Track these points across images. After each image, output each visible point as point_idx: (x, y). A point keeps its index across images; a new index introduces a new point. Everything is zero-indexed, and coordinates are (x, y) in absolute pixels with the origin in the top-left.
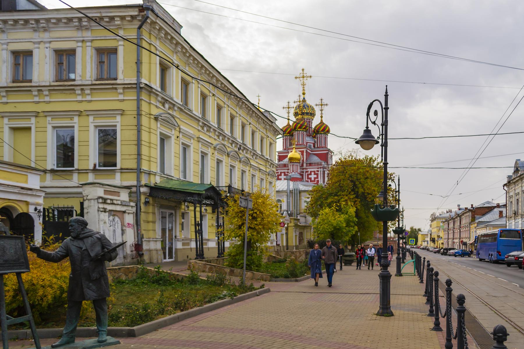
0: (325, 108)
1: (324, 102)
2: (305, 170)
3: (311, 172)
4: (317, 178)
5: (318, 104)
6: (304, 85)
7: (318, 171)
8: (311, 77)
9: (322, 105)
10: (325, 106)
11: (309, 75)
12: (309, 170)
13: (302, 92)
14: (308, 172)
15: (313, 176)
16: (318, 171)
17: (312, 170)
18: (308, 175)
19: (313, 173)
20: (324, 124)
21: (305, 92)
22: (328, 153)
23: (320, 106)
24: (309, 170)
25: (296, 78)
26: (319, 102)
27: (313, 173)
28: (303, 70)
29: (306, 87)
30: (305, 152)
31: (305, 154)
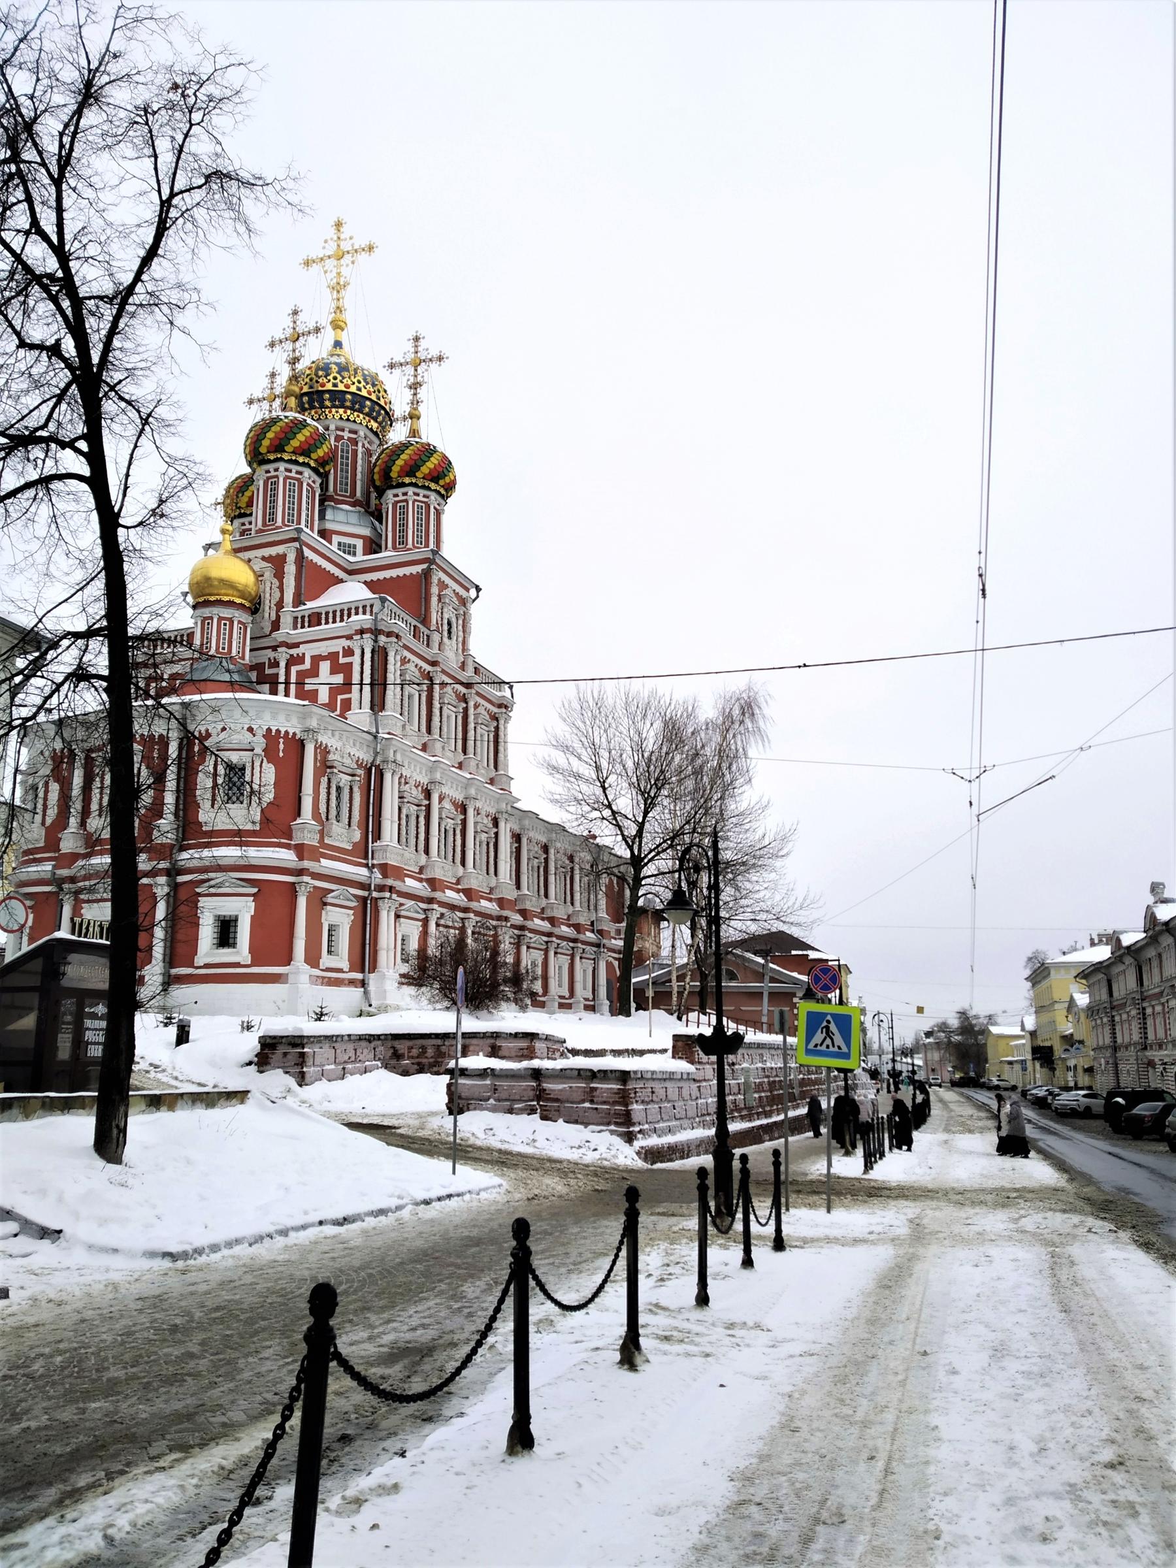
0: (431, 374)
1: (430, 347)
2: (283, 655)
3: (316, 659)
5: (399, 358)
6: (338, 288)
7: (349, 652)
8: (371, 248)
10: (434, 366)
11: (364, 243)
12: (308, 651)
14: (300, 660)
16: (349, 652)
17: (323, 648)
19: (325, 667)
21: (348, 316)
22: (427, 574)
23: (410, 370)
24: (308, 651)
26: (402, 350)
27: (325, 667)
28: (339, 225)
29: (348, 297)
30: (291, 557)
31: (290, 569)
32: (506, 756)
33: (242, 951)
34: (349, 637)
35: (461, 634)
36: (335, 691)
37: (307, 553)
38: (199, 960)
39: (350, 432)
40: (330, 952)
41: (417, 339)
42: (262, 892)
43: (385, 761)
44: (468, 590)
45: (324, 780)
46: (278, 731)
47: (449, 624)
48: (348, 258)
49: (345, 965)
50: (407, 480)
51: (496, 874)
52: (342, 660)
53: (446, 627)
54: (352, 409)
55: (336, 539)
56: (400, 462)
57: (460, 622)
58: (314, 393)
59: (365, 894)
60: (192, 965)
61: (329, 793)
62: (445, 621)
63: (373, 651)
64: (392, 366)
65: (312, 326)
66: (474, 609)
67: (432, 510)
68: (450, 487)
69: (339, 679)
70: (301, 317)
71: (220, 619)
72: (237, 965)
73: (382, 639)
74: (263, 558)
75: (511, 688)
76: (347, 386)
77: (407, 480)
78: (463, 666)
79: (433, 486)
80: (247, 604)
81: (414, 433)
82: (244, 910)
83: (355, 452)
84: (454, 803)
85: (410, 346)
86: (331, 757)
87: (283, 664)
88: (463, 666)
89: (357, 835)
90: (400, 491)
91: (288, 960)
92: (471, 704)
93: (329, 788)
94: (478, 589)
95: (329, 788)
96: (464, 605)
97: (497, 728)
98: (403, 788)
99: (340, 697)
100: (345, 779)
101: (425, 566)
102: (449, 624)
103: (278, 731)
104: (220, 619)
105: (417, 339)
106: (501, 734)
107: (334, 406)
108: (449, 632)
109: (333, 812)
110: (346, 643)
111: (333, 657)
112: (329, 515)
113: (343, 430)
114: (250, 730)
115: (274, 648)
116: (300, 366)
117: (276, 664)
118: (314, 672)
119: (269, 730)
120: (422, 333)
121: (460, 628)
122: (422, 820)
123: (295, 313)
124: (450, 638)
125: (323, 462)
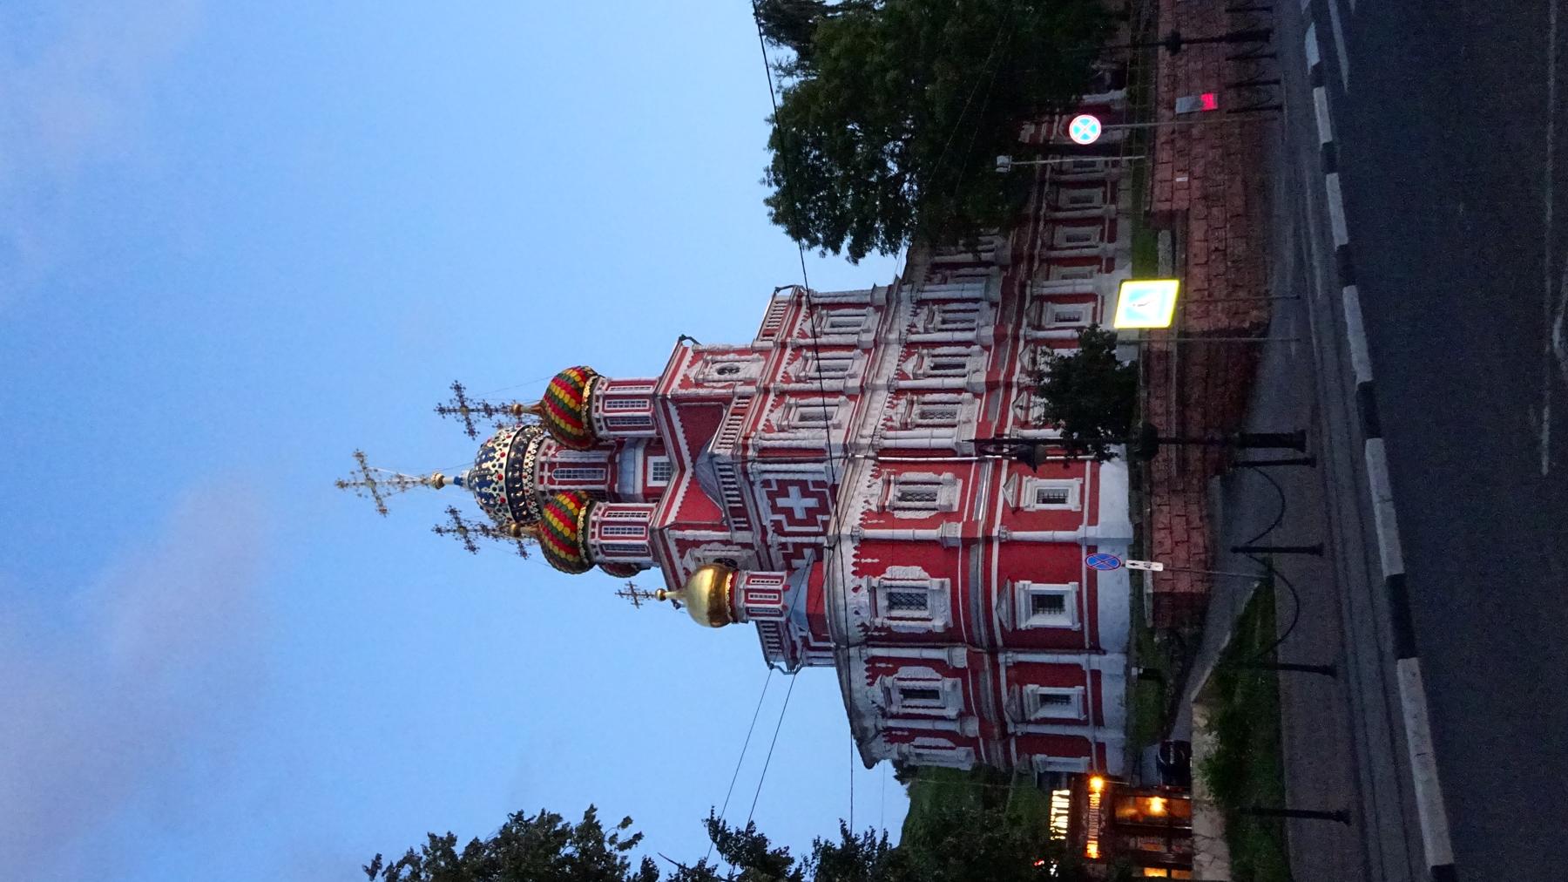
0: (474, 396)
1: (448, 398)
2: (772, 538)
3: (775, 509)
4: (802, 484)
5: (463, 426)
9: (465, 410)
10: (466, 394)
12: (768, 518)
13: (433, 489)
14: (777, 524)
15: (797, 503)
17: (764, 504)
18: (792, 521)
20: (541, 404)
22: (677, 400)
23: (473, 416)
25: (384, 511)
26: (455, 424)
30: (679, 534)
31: (689, 534)
32: (851, 294)
33: (1069, 588)
34: (752, 484)
35: (731, 356)
36: (805, 493)
37: (671, 519)
38: (1077, 626)
39: (542, 469)
40: (1063, 501)
41: (442, 410)
42: (1010, 574)
43: (871, 446)
44: (686, 349)
45: (899, 514)
46: (854, 564)
47: (721, 371)
48: (372, 475)
49: (1075, 483)
50: (584, 420)
51: (976, 300)
52: (775, 488)
53: (727, 376)
54: (521, 470)
55: (652, 483)
56: (569, 428)
57: (719, 358)
58: (515, 506)
59: (1005, 462)
60: (1081, 632)
61: (909, 509)
62: (722, 377)
63: (765, 463)
64: (472, 432)
65: (449, 517)
66: (705, 344)
67: (609, 392)
68: (585, 374)
69: (794, 490)
70: (443, 525)
71: (747, 601)
72: (1079, 594)
73: (751, 453)
74: (682, 557)
75: (778, 290)
76: (500, 478)
77: (584, 420)
78: (765, 352)
79: (586, 393)
80: (730, 577)
81: (533, 411)
82: (1026, 587)
83: (562, 464)
84: (905, 357)
85: (450, 417)
86: (874, 508)
87: (783, 540)
88: (765, 352)
89: (948, 476)
90: (597, 425)
91: (1074, 545)
92: (802, 341)
93: (904, 509)
94: (683, 338)
95: (904, 509)
96: (702, 352)
97: (824, 306)
98: (897, 425)
99: (812, 489)
100: (894, 491)
101: (670, 404)
102: (721, 371)
103: (854, 564)
104: (747, 601)
105: (442, 410)
106: (828, 300)
107: (521, 488)
108: (731, 371)
109: (930, 504)
110: (757, 488)
111: (772, 496)
112: (629, 490)
113: (542, 478)
114: (855, 590)
115: (768, 547)
116: (491, 525)
117: (784, 546)
118: (789, 512)
119: (854, 573)
120: (435, 406)
121: (725, 358)
122: (929, 397)
123: (439, 530)
124: (737, 370)
125: (579, 503)
